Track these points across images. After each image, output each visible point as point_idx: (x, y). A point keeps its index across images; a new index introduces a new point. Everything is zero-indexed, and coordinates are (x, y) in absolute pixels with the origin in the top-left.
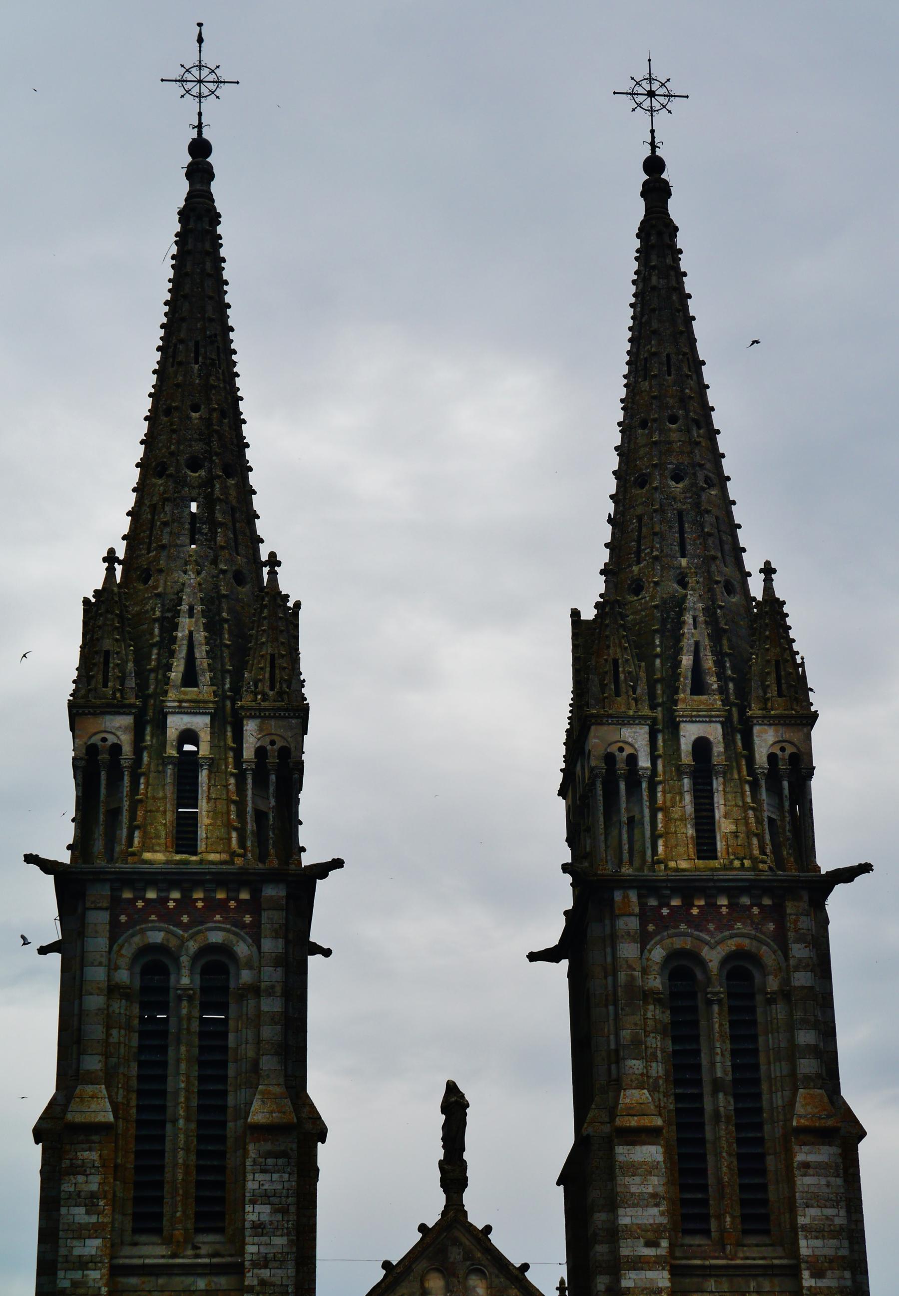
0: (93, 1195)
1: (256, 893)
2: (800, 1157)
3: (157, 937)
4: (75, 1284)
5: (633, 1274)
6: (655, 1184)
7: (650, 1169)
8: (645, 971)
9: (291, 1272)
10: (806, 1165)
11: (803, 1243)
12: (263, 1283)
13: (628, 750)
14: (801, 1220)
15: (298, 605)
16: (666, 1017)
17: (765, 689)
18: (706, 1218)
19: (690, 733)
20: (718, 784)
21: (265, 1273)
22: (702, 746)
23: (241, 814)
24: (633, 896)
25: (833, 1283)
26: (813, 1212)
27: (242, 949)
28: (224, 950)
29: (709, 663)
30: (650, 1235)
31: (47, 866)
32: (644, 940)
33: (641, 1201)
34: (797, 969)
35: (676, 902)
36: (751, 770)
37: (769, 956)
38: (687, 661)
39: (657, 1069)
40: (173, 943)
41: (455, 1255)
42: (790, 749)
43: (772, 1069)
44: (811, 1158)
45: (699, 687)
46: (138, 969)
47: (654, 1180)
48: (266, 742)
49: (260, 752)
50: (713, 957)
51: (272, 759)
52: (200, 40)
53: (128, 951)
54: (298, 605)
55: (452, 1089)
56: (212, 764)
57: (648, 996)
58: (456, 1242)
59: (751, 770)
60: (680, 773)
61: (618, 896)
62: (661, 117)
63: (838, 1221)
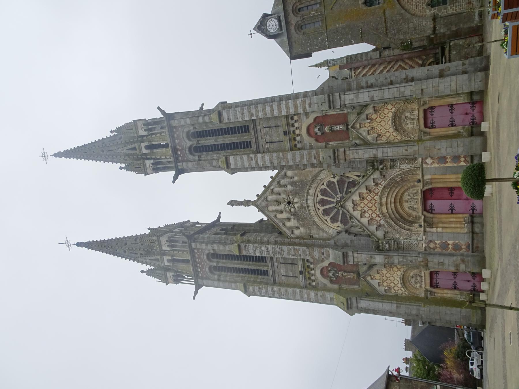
0: (259, 288)
1: (194, 249)
2: (227, 121)
3: (207, 269)
4: (278, 293)
5: (259, 163)
6: (238, 158)
7: (235, 160)
8: (195, 161)
9: (269, 246)
10: (228, 119)
11: (246, 119)
12: (273, 253)
13: (151, 165)
14: (241, 120)
15: (149, 229)
16: (205, 153)
17: (131, 133)
18: (247, 142)
19: (145, 151)
20: (154, 143)
21: (271, 252)
22: (147, 147)
23: (181, 251)
24: (179, 164)
25: (254, 110)
26: (238, 117)
27: (207, 252)
28: (208, 255)
29: (130, 147)
30: (250, 159)
31: (196, 292)
32: (188, 161)
33: (243, 162)
34: (186, 123)
35: (179, 153)
36: (149, 135)
37: (186, 130)
38: (130, 152)
39: (215, 157)
40: (208, 266)
41: (263, 204)
42: (142, 126)
43: (210, 127)
44: (226, 118)
45: (135, 149)
46: (215, 272)
47: (237, 158)
48: (166, 245)
49: (168, 246)
50: (189, 143)
51: (168, 243)
52: (62, 244)
53: (211, 275)
54: (149, 229)
55: (228, 204)
56: (172, 256)
57: (199, 160)
58: (260, 204)
59: (149, 135)
60: (152, 153)
61: (180, 168)
62: (49, 154)
63: (240, 110)
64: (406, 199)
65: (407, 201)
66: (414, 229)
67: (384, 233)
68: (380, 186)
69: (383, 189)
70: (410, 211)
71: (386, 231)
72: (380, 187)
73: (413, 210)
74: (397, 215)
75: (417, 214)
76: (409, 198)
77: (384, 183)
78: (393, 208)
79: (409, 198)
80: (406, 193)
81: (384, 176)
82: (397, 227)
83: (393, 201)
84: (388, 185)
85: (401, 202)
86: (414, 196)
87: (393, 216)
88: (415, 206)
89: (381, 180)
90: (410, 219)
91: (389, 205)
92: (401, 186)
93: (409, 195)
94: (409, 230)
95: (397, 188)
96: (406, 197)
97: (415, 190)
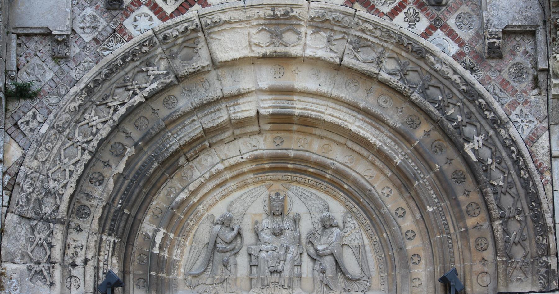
64: (296, 206)
65: (277, 210)
66: (85, 239)
67: (60, 28)
68: (423, 24)
69: (402, 42)
70: (203, 232)
71: (75, 49)
72: (412, 21)
73: (213, 247)
74: (192, 129)
75: (179, 274)
76: (305, 226)
77: (443, 47)
78: (246, 109)
79: (305, 226)
80: (337, 209)
81: (495, 53)
82: (99, 122)
83: (299, 107)
84: (435, 79)
85: (278, 165)
86: (316, 257)
87: (184, 103)
88: (242, 260)
89: (466, 35)
90: (147, 227)
91: (266, 77)
92: (413, 166)
93: (327, 225)
94: (78, 209)
95: (402, 136)
96: (308, 204)
97: (362, 262)
